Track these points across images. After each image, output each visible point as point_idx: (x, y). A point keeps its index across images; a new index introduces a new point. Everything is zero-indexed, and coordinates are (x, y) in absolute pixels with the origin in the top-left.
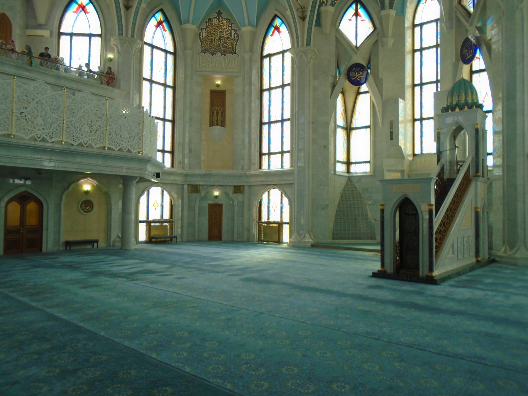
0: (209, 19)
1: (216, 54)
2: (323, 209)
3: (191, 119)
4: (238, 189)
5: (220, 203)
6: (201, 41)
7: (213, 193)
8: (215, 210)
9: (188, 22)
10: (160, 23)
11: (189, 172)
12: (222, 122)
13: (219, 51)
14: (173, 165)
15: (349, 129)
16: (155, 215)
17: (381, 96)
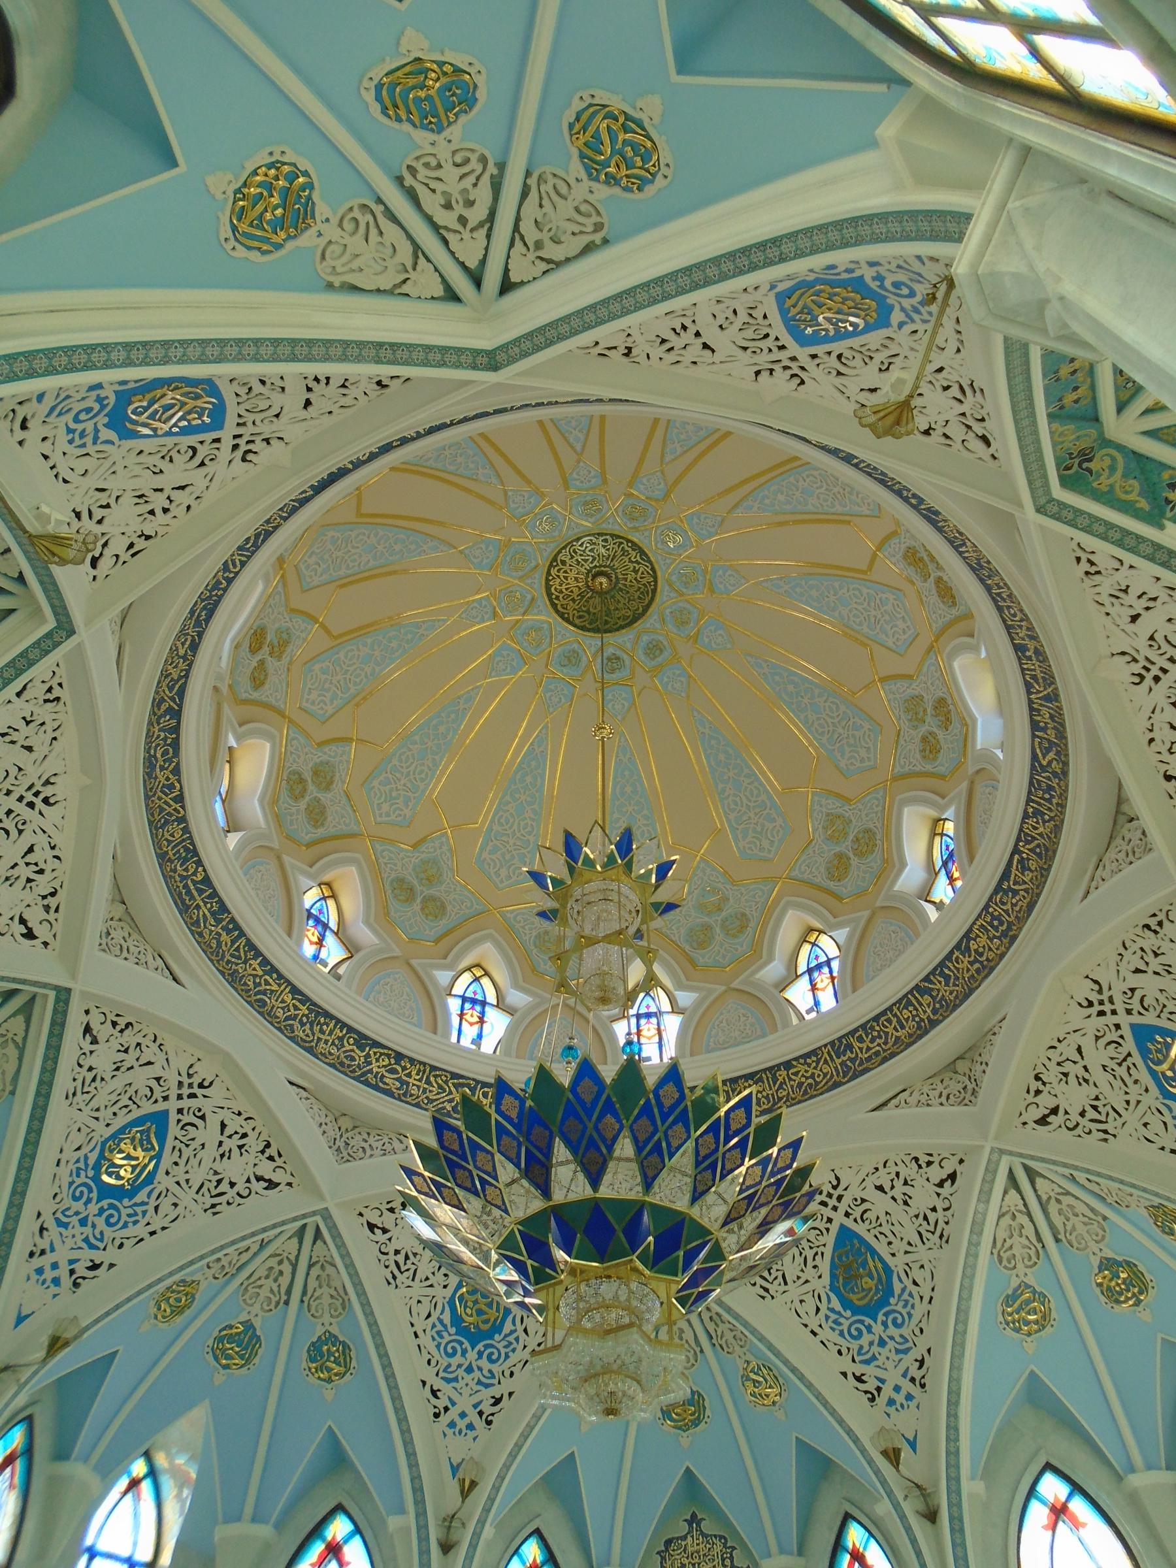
9: (1132, 1469)
10: (1059, 1511)
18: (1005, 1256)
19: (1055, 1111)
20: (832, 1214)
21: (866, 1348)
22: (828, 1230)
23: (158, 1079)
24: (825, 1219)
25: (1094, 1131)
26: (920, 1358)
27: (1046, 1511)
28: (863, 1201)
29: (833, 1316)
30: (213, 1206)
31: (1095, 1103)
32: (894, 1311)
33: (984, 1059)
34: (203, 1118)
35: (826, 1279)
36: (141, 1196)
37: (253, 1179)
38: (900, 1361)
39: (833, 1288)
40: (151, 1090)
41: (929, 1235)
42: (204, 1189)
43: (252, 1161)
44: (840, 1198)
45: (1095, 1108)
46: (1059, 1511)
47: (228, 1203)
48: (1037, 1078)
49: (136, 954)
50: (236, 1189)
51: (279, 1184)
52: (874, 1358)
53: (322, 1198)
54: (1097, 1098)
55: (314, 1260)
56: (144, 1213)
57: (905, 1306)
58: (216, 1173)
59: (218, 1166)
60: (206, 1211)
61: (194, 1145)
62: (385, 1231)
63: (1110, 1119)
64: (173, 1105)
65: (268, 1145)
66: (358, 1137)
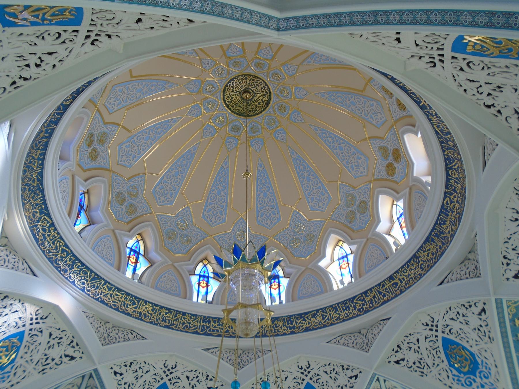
19: (403, 360)
22: (302, 383)
23: (20, 318)
28: (318, 375)
30: (43, 370)
31: (420, 361)
34: (41, 332)
36: (8, 369)
37: (63, 356)
40: (16, 323)
42: (40, 363)
43: (63, 350)
44: (309, 372)
45: (420, 363)
47: (51, 368)
48: (398, 346)
49: (13, 263)
50: (55, 362)
51: (76, 358)
53: (95, 364)
54: (421, 359)
55: (88, 385)
56: (9, 376)
58: (46, 355)
59: (47, 352)
60: (39, 372)
61: (36, 344)
62: (121, 374)
63: (425, 368)
64: (28, 327)
65: (72, 342)
66: (114, 332)
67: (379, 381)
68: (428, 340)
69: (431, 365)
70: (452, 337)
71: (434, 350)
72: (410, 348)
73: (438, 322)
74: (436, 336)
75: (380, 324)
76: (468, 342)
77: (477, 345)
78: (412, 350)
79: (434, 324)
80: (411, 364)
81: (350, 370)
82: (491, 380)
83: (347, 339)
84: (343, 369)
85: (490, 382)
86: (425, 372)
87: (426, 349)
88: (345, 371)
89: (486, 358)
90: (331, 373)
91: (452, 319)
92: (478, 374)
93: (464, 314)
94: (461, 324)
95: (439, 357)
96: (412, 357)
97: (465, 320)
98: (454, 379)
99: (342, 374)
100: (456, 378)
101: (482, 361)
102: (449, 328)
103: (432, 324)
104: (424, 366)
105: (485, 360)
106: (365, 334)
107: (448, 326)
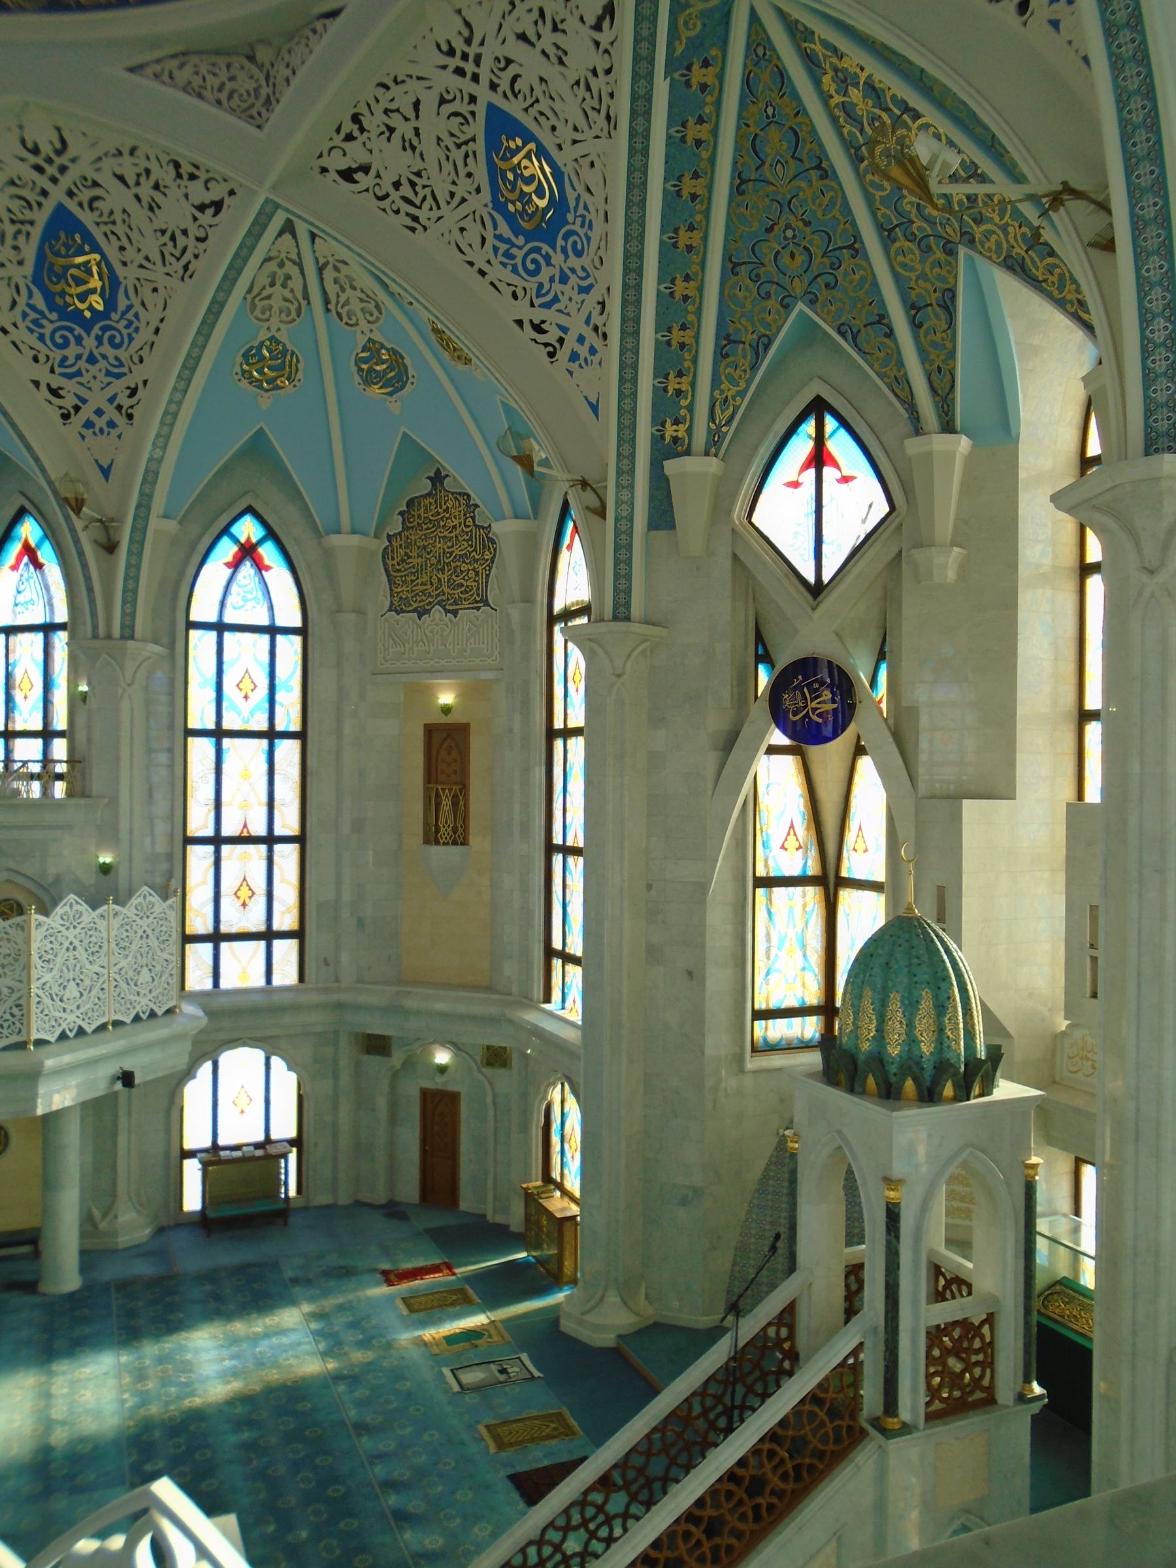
0: (410, 503)
1: (428, 612)
2: (684, 1202)
3: (358, 826)
4: (496, 1057)
5: (452, 1088)
6: (388, 575)
7: (433, 1055)
8: (439, 1110)
10: (247, 552)
11: (345, 997)
12: (455, 831)
13: (439, 603)
14: (301, 978)
15: (830, 882)
16: (241, 1129)
17: (912, 779)
18: (260, 304)
19: (365, 169)
20: (49, 186)
21: (71, 361)
24: (38, 190)
25: (402, 213)
26: (133, 386)
27: (235, 549)
28: (96, 184)
29: (33, 315)
32: (114, 329)
33: (295, 60)
35: (29, 268)
38: (109, 384)
39: (37, 280)
41: (173, 260)
44: (63, 169)
45: (413, 185)
46: (247, 552)
48: (356, 119)
52: (79, 373)
54: (418, 174)
57: (127, 327)
63: (426, 206)
67: (294, 236)
68: (447, 109)
69: (442, 197)
70: (514, 108)
71: (459, 146)
72: (391, 130)
73: (482, 44)
74: (473, 99)
75: (314, 31)
76: (554, 128)
77: (575, 142)
78: (396, 137)
79: (472, 51)
80: (387, 187)
81: (198, 185)
82: (585, 261)
83: (203, 70)
84: (179, 176)
85: (583, 269)
86: (423, 220)
87: (439, 139)
88: (185, 182)
89: (588, 190)
90: (138, 184)
91: (522, 37)
92: (560, 242)
93: (558, 21)
94: (544, 59)
95: (469, 175)
96: (392, 162)
97: (558, 47)
98: (496, 249)
99: (175, 192)
100: (503, 247)
101: (578, 199)
102: (512, 70)
103: (466, 49)
104: (424, 199)
105: (585, 196)
106: (267, 65)
107: (509, 62)
